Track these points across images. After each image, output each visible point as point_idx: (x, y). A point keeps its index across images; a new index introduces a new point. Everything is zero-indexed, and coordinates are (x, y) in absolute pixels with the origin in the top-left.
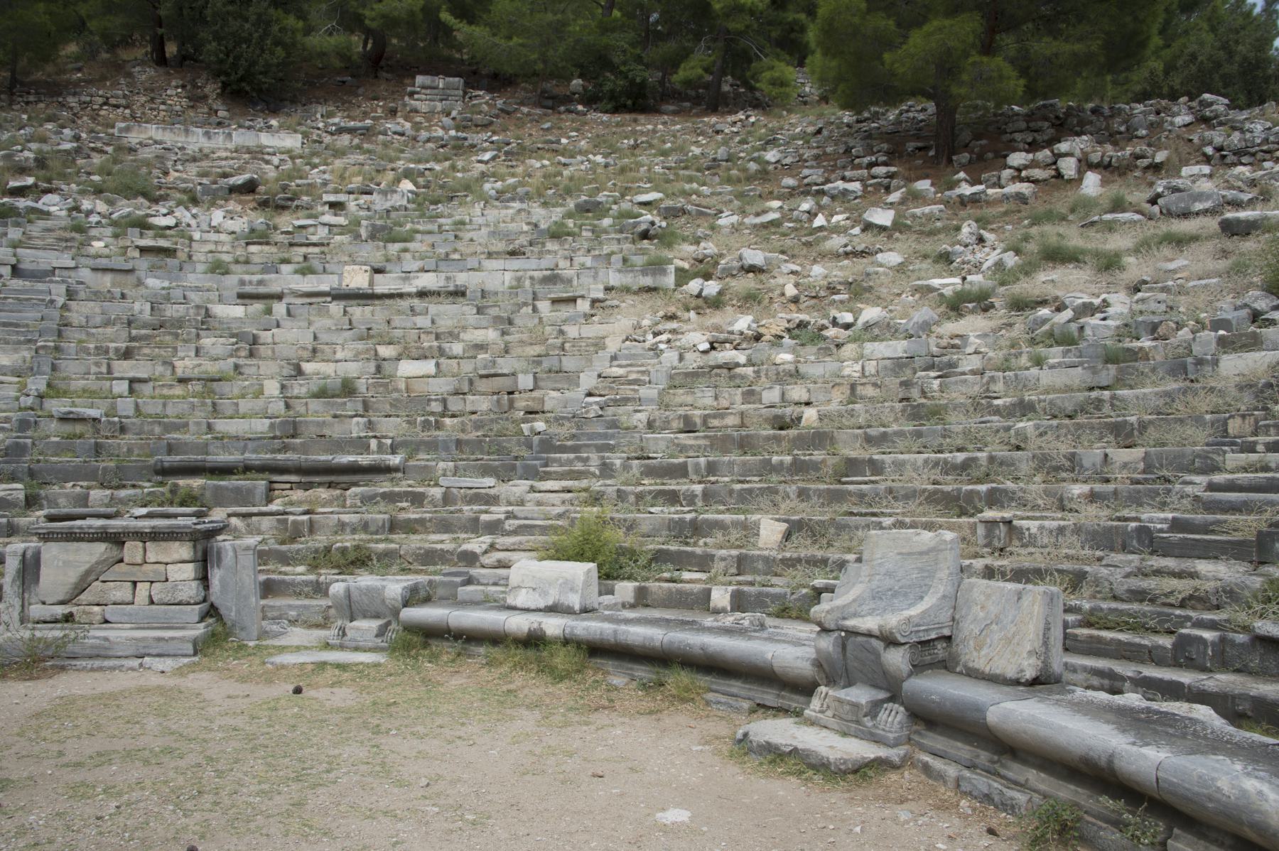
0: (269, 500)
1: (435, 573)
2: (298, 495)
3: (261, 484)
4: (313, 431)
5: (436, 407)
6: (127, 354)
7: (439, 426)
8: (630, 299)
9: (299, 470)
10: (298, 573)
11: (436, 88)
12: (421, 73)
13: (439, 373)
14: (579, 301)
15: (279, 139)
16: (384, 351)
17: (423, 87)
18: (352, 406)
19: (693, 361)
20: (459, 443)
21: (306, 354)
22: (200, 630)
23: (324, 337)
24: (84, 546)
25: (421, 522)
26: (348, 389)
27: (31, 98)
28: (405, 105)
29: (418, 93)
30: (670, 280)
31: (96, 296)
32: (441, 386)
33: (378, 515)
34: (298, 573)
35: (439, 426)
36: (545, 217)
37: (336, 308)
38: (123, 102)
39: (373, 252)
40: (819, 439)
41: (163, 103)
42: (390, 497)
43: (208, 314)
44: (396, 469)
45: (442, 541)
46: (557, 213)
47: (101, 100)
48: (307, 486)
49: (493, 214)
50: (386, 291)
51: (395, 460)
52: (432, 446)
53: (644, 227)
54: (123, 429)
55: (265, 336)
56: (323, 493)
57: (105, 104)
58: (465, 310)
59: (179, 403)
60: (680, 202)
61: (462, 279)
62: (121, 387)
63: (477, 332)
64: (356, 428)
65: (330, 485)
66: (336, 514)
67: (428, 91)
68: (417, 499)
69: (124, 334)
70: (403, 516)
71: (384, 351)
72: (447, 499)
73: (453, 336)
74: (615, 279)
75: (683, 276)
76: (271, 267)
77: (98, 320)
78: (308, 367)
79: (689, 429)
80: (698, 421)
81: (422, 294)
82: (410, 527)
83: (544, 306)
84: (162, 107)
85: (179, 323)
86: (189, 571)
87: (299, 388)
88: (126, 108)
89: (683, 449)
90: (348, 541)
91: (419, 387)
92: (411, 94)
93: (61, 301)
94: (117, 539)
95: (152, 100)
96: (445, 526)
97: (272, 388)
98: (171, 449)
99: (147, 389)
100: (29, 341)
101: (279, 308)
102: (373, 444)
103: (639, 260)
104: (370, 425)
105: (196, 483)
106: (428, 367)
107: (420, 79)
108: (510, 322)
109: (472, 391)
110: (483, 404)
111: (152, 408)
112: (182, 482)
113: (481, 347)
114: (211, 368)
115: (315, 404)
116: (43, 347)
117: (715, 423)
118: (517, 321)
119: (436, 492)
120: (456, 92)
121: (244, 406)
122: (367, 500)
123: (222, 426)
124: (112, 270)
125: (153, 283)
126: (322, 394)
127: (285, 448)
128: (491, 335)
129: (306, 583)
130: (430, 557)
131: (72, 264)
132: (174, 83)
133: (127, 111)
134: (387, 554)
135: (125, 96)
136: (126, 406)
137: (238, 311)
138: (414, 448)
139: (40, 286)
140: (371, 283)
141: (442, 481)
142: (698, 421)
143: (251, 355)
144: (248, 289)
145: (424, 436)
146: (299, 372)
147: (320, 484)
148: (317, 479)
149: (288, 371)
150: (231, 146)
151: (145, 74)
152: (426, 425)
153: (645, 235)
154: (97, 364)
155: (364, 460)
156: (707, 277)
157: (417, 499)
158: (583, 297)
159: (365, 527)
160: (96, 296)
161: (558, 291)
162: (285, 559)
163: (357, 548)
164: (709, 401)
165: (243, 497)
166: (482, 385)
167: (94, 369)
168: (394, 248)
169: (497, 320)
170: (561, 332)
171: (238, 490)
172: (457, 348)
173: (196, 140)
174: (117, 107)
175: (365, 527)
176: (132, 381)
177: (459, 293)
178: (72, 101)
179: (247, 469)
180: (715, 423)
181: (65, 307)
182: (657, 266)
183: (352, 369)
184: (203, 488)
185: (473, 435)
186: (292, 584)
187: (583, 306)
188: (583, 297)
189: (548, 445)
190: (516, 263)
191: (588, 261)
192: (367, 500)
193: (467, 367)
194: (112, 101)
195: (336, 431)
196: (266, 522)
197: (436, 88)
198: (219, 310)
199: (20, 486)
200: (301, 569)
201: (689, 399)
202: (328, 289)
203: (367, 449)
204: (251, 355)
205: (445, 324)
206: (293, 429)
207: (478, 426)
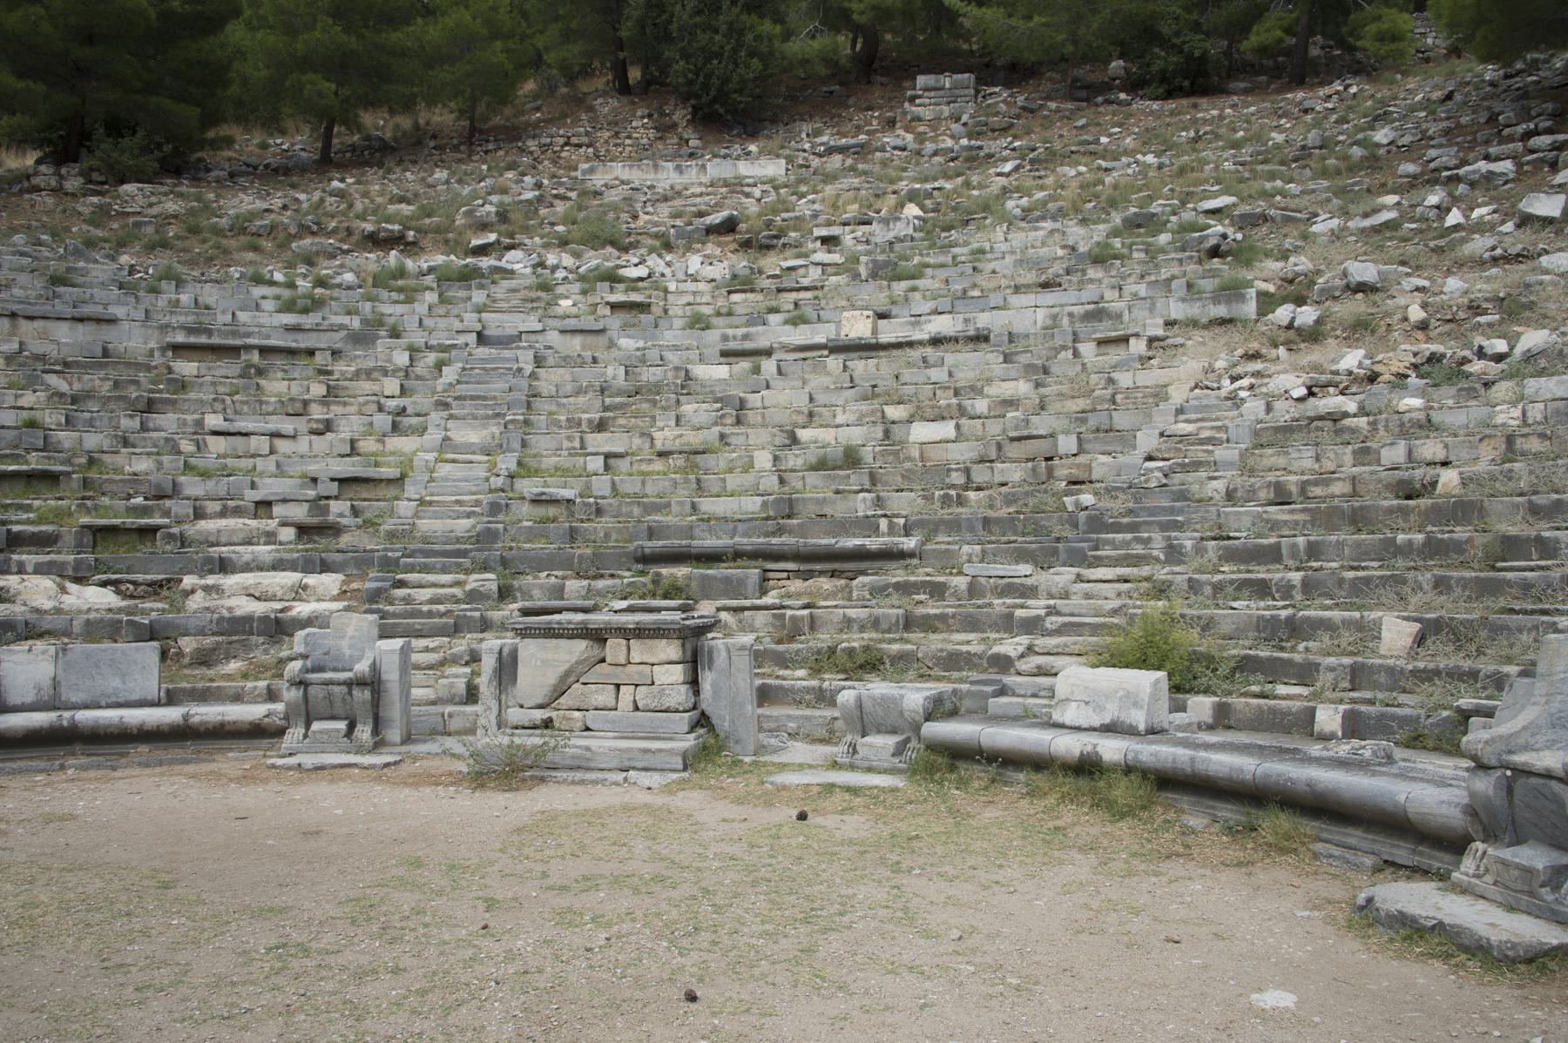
0: (763, 592)
1: (961, 681)
2: (796, 585)
3: (754, 574)
4: (812, 509)
5: (957, 478)
6: (601, 426)
7: (961, 501)
8: (1198, 335)
10: (798, 678)
11: (942, 88)
12: (923, 73)
13: (960, 436)
14: (1132, 341)
15: (759, 167)
16: (893, 412)
17: (926, 89)
18: (856, 479)
19: (1285, 412)
20: (986, 522)
21: (801, 419)
22: (689, 742)
23: (821, 398)
24: (562, 642)
25: (942, 618)
26: (851, 459)
27: (491, 146)
28: (905, 113)
29: (920, 97)
30: (1250, 308)
31: (566, 361)
32: (963, 453)
33: (891, 610)
34: (798, 678)
35: (961, 501)
36: (1084, 237)
37: (834, 363)
38: (585, 140)
39: (876, 294)
40: (1462, 510)
41: (629, 137)
42: (905, 588)
43: (688, 376)
44: (911, 555)
45: (969, 643)
46: (1099, 231)
47: (561, 141)
48: (807, 576)
49: (1018, 238)
50: (893, 340)
51: (910, 543)
52: (954, 526)
53: (1213, 241)
54: (599, 512)
55: (754, 400)
56: (825, 584)
57: (567, 144)
58: (988, 359)
59: (659, 480)
60: (1260, 206)
61: (984, 320)
62: (596, 464)
63: (1005, 385)
64: (862, 505)
65: (833, 574)
66: (842, 610)
67: (932, 94)
68: (937, 591)
69: (598, 404)
70: (921, 611)
71: (893, 412)
72: (974, 590)
73: (976, 390)
74: (1177, 310)
75: (1267, 302)
76: (757, 319)
77: (569, 388)
78: (803, 435)
79: (1282, 498)
80: (1294, 489)
81: (936, 341)
82: (929, 625)
83: (1087, 349)
84: (628, 142)
85: (657, 388)
86: (677, 673)
87: (794, 460)
88: (588, 146)
89: (1274, 526)
90: (855, 640)
91: (936, 455)
92: (912, 100)
93: (529, 368)
94: (599, 636)
95: (617, 134)
96: (971, 624)
97: (763, 460)
98: (652, 533)
99: (623, 465)
100: (498, 415)
101: (769, 366)
102: (883, 524)
103: (1208, 285)
104: (879, 502)
105: (681, 571)
106: (947, 429)
107: (921, 80)
108: (1046, 371)
109: (1001, 458)
110: (1015, 473)
111: (630, 486)
113: (1011, 403)
114: (694, 439)
115: (813, 478)
116: (512, 421)
117: (1318, 491)
118: (1055, 369)
119: (961, 582)
120: (966, 92)
121: (733, 481)
122: (877, 591)
123: (708, 505)
124: (582, 331)
125: (627, 343)
126: (821, 465)
127: (780, 531)
128: (1023, 388)
129: (808, 690)
130: (954, 661)
131: (539, 327)
132: (639, 113)
133: (590, 150)
134: (902, 657)
135: (587, 134)
136: (601, 485)
137: (722, 371)
138: (932, 528)
139: (507, 354)
140: (875, 331)
141: (967, 568)
142: (1294, 489)
143: (739, 422)
144: (733, 345)
145: (944, 513)
146: (794, 440)
147: (821, 573)
148: (818, 567)
149: (781, 439)
150: (705, 179)
151: (607, 106)
153: (1215, 252)
154: (570, 438)
155: (873, 543)
156: (1300, 301)
157: (937, 591)
158: (1137, 335)
159: (875, 623)
160: (566, 361)
161: (1105, 330)
162: (783, 661)
163: (867, 649)
164: (1308, 463)
165: (733, 588)
166: (1013, 450)
167: (566, 444)
168: (900, 287)
170: (1111, 381)
171: (727, 580)
172: (981, 406)
173: (667, 176)
174: (579, 146)
175: (875, 623)
176: (607, 456)
177: (981, 338)
178: (532, 145)
179: (738, 555)
180: (1318, 491)
181: (533, 376)
182: (1232, 292)
183: (855, 435)
184: (689, 578)
185: (1004, 512)
186: (792, 690)
187: (1138, 347)
188: (1137, 335)
189: (1098, 523)
190: (1050, 297)
191: (1142, 290)
192: (877, 591)
193: (994, 428)
194: (574, 140)
195: (839, 509)
196: (761, 618)
197: (942, 88)
198: (701, 371)
199: (492, 576)
200: (801, 673)
201: (1281, 461)
202: (823, 341)
204: (739, 422)
205: (964, 377)
206: (788, 508)
207: (1009, 500)
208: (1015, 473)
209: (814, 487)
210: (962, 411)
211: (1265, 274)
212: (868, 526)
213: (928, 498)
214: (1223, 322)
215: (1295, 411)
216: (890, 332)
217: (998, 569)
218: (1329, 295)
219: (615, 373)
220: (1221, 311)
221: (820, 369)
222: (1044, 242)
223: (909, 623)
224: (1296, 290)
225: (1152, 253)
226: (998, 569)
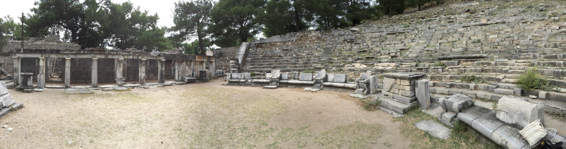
0: (458, 64)
1: (490, 84)
2: (465, 63)
3: (456, 62)
4: (470, 50)
5: (497, 44)
7: (496, 48)
8: (538, 22)
9: (465, 58)
10: (458, 82)
13: (498, 37)
16: (487, 34)
18: (480, 44)
19: (555, 32)
20: (500, 51)
25: (489, 70)
26: (479, 41)
30: (547, 18)
31: (440, 30)
32: (498, 40)
33: (479, 68)
34: (458, 82)
35: (496, 48)
36: (521, 10)
37: (479, 27)
39: (488, 18)
42: (483, 64)
44: (485, 57)
45: (492, 75)
46: (524, 9)
49: (512, 10)
51: (485, 55)
52: (494, 52)
55: (465, 33)
56: (469, 63)
60: (548, 5)
61: (505, 20)
62: (438, 44)
64: (479, 49)
65: (471, 61)
66: (470, 68)
68: (489, 64)
70: (485, 68)
71: (487, 34)
72: (496, 64)
73: (502, 30)
74: (535, 18)
75: (550, 17)
76: (469, 22)
78: (472, 38)
79: (556, 46)
80: (558, 45)
81: (496, 23)
82: (486, 71)
83: (521, 24)
87: (469, 42)
89: (554, 51)
90: (471, 74)
91: (493, 40)
96: (494, 71)
97: (464, 42)
98: (443, 55)
99: (442, 44)
101: (469, 28)
102: (481, 52)
103: (540, 15)
105: (444, 61)
106: (496, 36)
109: (505, 40)
110: (506, 43)
111: (442, 47)
112: (442, 61)
113: (507, 32)
115: (472, 45)
117: (563, 45)
119: (493, 63)
122: (478, 64)
123: (453, 50)
125: (449, 27)
126: (474, 42)
127: (464, 53)
128: (510, 30)
129: (459, 85)
130: (490, 79)
134: (479, 78)
136: (438, 48)
138: (491, 52)
141: (495, 60)
142: (558, 45)
145: (493, 50)
146: (470, 39)
152: (494, 47)
153: (541, 10)
155: (478, 55)
156: (555, 16)
157: (489, 64)
159: (476, 71)
160: (440, 30)
161: (523, 21)
162: (457, 78)
163: (473, 76)
164: (560, 40)
165: (453, 64)
166: (507, 39)
168: (492, 16)
169: (511, 27)
171: (452, 63)
172: (503, 32)
175: (476, 71)
177: (504, 23)
179: (455, 58)
180: (563, 45)
182: (544, 15)
183: (480, 38)
185: (504, 50)
186: (456, 85)
187: (529, 23)
189: (520, 51)
190: (516, 17)
191: (530, 16)
192: (478, 64)
193: (504, 36)
195: (475, 49)
196: (456, 70)
198: (459, 30)
200: (460, 81)
201: (555, 40)
203: (480, 53)
205: (500, 28)
206: (466, 50)
207: (505, 48)
208: (506, 43)
209: (471, 46)
210: (499, 33)
211: (549, 13)
212: (479, 52)
213: (490, 47)
214: (542, 20)
215: (557, 31)
216: (489, 22)
217: (501, 60)
218: (560, 15)
219: (445, 31)
220: (542, 18)
221: (477, 28)
222: (515, 10)
223: (482, 71)
224: (554, 15)
225: (531, 11)
226: (501, 60)
